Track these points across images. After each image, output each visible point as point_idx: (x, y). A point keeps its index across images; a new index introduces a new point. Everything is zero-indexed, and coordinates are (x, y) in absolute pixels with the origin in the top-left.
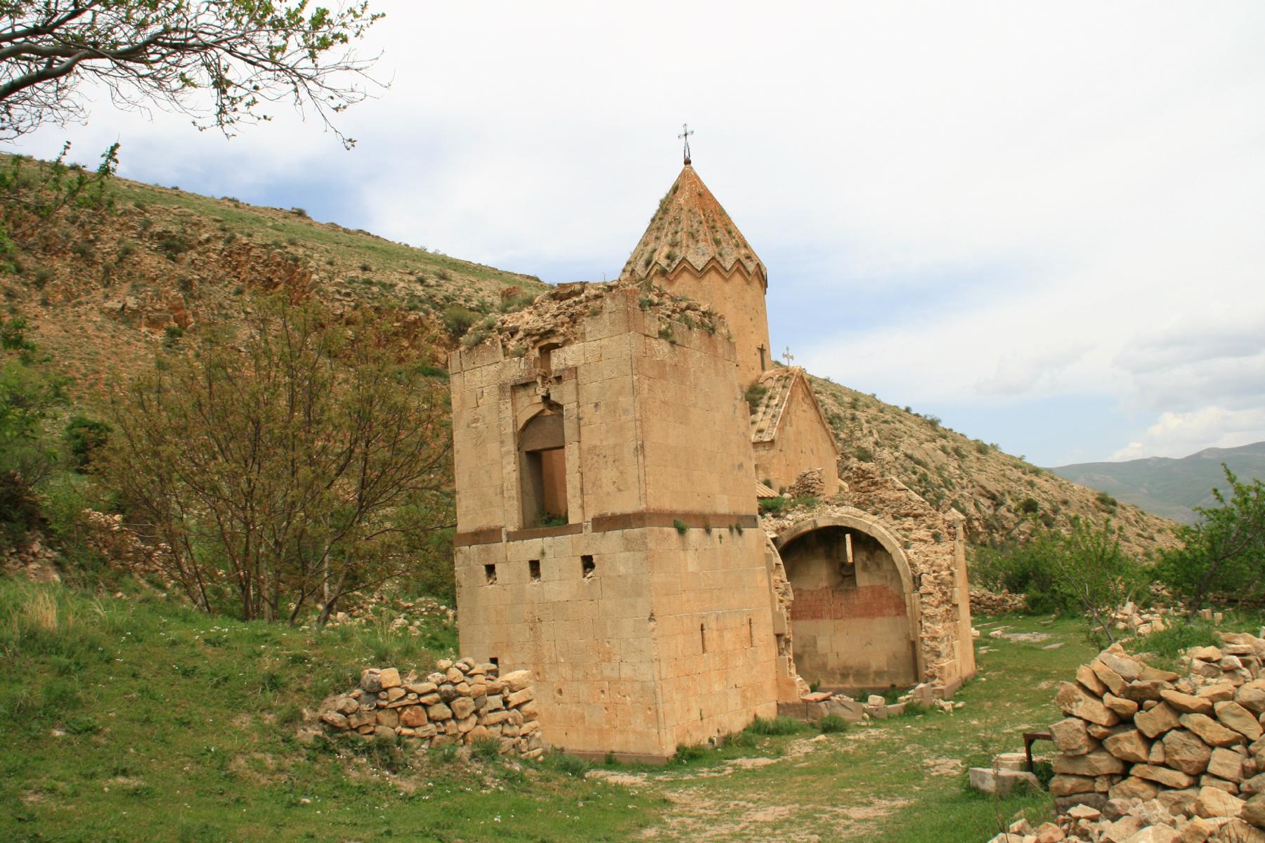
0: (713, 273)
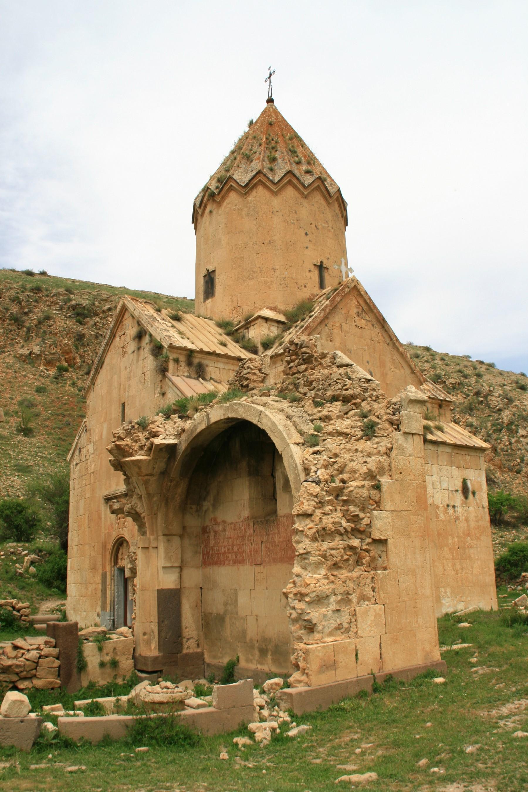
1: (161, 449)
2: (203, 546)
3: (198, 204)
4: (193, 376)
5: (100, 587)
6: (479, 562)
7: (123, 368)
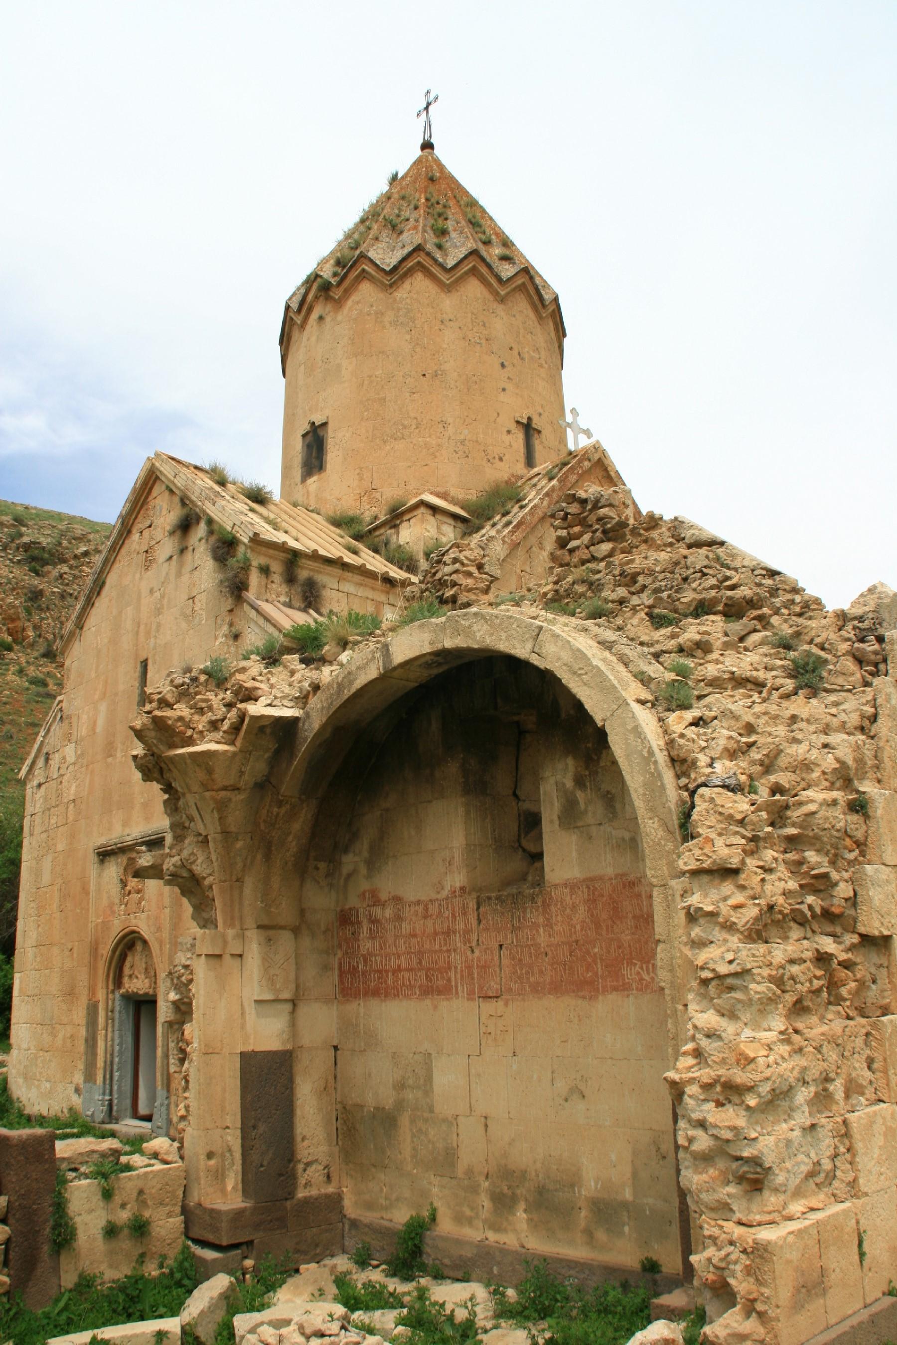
0: (419, 276)
1: (262, 729)
2: (340, 954)
3: (295, 306)
4: (297, 603)
5: (83, 1032)
7: (145, 592)
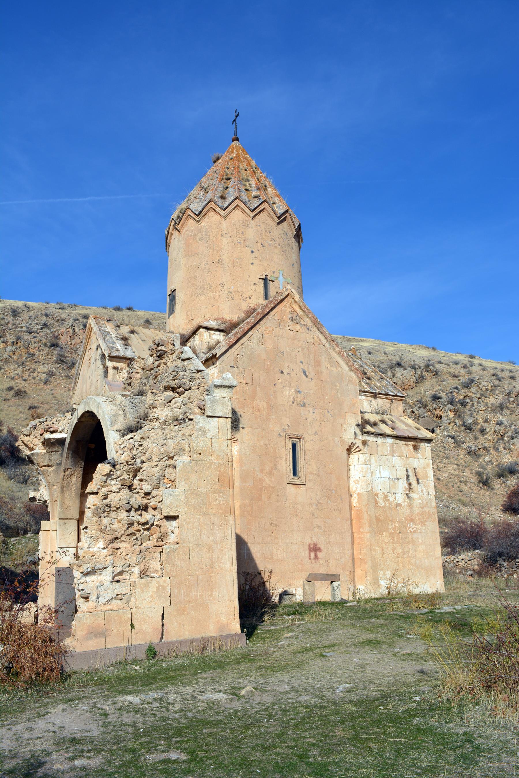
6: (424, 546)
